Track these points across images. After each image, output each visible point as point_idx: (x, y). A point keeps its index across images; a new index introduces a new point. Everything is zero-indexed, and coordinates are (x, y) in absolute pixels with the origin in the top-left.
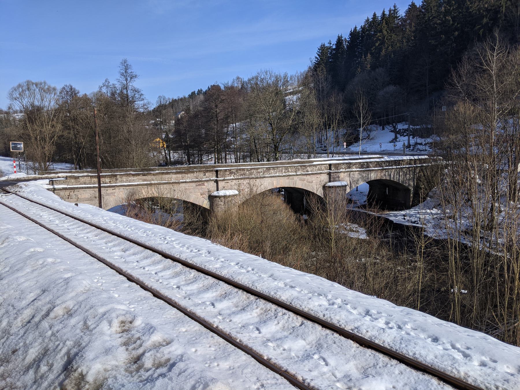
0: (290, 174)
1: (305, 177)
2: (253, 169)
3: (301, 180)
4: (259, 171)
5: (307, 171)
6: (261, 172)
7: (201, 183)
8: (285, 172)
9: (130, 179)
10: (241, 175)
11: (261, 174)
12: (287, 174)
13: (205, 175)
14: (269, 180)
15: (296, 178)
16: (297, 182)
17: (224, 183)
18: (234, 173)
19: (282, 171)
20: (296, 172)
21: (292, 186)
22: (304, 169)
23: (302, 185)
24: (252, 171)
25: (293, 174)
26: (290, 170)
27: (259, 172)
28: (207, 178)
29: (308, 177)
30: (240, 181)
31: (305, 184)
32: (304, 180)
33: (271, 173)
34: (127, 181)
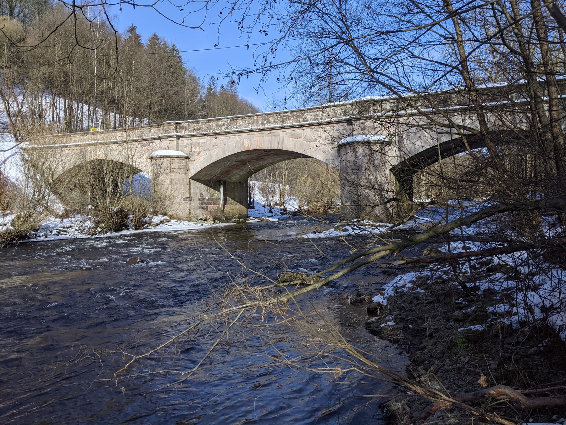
0: (272, 126)
1: (299, 131)
2: (211, 120)
3: (292, 136)
4: (220, 123)
5: (305, 120)
6: (224, 125)
7: (145, 142)
8: (262, 124)
9: (82, 138)
10: (195, 130)
11: (224, 127)
12: (266, 126)
13: (150, 132)
14: (237, 137)
15: (283, 133)
16: (285, 141)
17: (168, 142)
18: (186, 128)
19: (257, 123)
20: (283, 122)
21: (276, 147)
22: (298, 117)
23: (295, 145)
24: (210, 124)
25: (277, 125)
26: (271, 119)
27: (221, 126)
28: (152, 135)
29: (307, 131)
30: (194, 140)
31: (301, 145)
32: (298, 137)
33: (240, 126)
34: (81, 141)
